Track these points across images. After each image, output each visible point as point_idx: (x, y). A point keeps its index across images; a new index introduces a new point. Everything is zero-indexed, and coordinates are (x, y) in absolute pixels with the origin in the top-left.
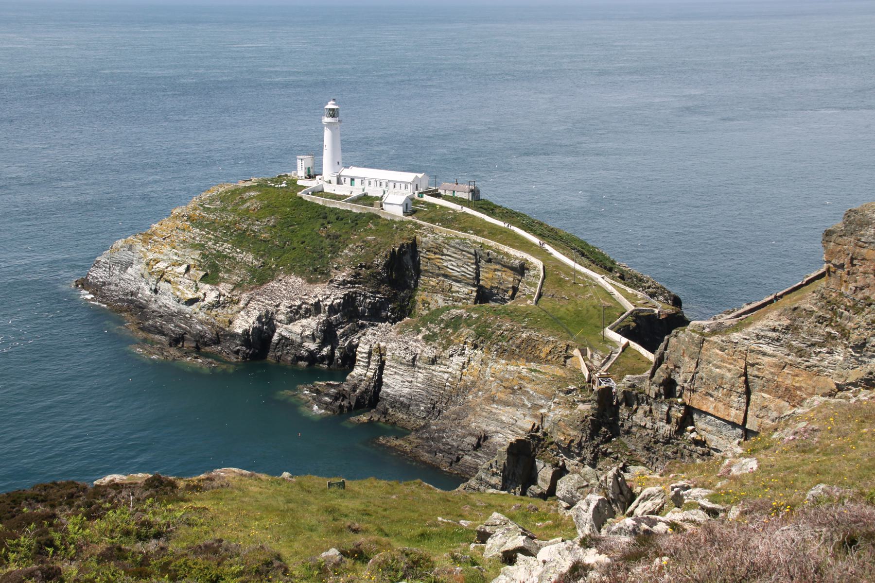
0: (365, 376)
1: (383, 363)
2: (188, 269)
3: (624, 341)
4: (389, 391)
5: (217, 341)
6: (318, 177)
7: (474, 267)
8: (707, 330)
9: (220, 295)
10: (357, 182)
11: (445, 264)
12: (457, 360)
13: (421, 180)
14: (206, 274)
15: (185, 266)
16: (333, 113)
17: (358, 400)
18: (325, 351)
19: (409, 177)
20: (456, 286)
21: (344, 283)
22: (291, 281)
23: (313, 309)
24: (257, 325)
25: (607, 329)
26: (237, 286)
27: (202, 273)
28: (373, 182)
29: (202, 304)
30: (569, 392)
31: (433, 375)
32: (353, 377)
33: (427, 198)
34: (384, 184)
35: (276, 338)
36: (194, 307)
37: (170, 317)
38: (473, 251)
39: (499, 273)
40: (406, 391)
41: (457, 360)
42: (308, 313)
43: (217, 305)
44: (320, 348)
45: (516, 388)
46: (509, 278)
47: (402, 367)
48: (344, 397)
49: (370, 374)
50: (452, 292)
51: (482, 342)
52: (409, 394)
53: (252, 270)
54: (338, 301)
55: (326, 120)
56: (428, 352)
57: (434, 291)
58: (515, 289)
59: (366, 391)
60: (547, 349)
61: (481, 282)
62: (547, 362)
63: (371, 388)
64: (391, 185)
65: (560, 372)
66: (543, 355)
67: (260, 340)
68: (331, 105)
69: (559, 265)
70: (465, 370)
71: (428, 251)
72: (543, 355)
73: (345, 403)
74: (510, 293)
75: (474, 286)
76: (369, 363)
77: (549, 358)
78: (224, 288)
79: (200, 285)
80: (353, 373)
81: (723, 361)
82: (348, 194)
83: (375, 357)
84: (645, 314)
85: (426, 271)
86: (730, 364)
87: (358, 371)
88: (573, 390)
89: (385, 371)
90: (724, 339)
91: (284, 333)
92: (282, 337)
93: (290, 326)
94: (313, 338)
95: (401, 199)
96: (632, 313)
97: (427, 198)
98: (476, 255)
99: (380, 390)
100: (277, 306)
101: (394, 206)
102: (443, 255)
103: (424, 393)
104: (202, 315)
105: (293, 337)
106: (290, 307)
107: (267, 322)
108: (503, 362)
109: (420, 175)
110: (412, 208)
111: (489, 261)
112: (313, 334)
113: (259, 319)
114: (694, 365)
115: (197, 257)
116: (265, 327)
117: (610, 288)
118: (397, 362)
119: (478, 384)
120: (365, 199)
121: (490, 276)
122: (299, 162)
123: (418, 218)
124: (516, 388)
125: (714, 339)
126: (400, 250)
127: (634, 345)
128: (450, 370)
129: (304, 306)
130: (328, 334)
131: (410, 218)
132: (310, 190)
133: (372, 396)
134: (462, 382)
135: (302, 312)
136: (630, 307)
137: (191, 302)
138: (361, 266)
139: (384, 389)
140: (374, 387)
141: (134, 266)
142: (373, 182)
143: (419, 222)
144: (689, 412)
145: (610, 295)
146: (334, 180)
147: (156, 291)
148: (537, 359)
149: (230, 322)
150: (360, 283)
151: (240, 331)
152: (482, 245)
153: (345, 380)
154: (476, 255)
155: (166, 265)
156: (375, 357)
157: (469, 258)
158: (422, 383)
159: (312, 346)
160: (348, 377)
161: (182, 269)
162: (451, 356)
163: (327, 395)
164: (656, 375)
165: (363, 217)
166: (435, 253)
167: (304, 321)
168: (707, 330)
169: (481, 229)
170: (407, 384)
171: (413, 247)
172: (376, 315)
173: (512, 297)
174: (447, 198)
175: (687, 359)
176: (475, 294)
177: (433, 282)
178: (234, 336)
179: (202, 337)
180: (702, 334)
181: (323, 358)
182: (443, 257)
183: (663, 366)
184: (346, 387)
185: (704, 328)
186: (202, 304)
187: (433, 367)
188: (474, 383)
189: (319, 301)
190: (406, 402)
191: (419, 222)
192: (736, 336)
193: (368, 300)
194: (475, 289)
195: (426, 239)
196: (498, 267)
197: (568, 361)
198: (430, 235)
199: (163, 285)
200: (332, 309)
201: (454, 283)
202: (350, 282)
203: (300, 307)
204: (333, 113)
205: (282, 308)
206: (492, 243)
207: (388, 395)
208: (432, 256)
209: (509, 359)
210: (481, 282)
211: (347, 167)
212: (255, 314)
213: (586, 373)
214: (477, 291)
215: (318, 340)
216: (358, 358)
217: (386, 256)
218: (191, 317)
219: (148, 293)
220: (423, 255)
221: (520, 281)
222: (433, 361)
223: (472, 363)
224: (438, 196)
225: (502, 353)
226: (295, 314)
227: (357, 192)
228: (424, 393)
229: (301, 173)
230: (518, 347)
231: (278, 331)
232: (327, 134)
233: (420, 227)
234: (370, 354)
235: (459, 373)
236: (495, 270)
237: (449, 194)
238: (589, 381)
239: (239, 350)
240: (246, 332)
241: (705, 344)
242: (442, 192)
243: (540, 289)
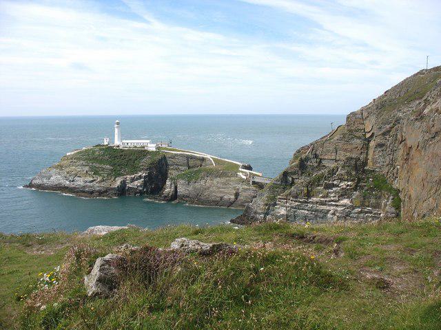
3: (248, 171)
5: (106, 191)
10: (129, 144)
16: (118, 124)
20: (180, 167)
35: (127, 188)
36: (94, 183)
42: (137, 179)
44: (143, 189)
46: (199, 162)
68: (117, 121)
87: (167, 190)
92: (129, 187)
94: (141, 186)
101: (152, 147)
107: (124, 183)
127: (250, 171)
133: (175, 196)
137: (92, 181)
144: (321, 159)
159: (141, 189)
165: (143, 153)
171: (165, 157)
195: (167, 156)
204: (118, 124)
232: (116, 130)
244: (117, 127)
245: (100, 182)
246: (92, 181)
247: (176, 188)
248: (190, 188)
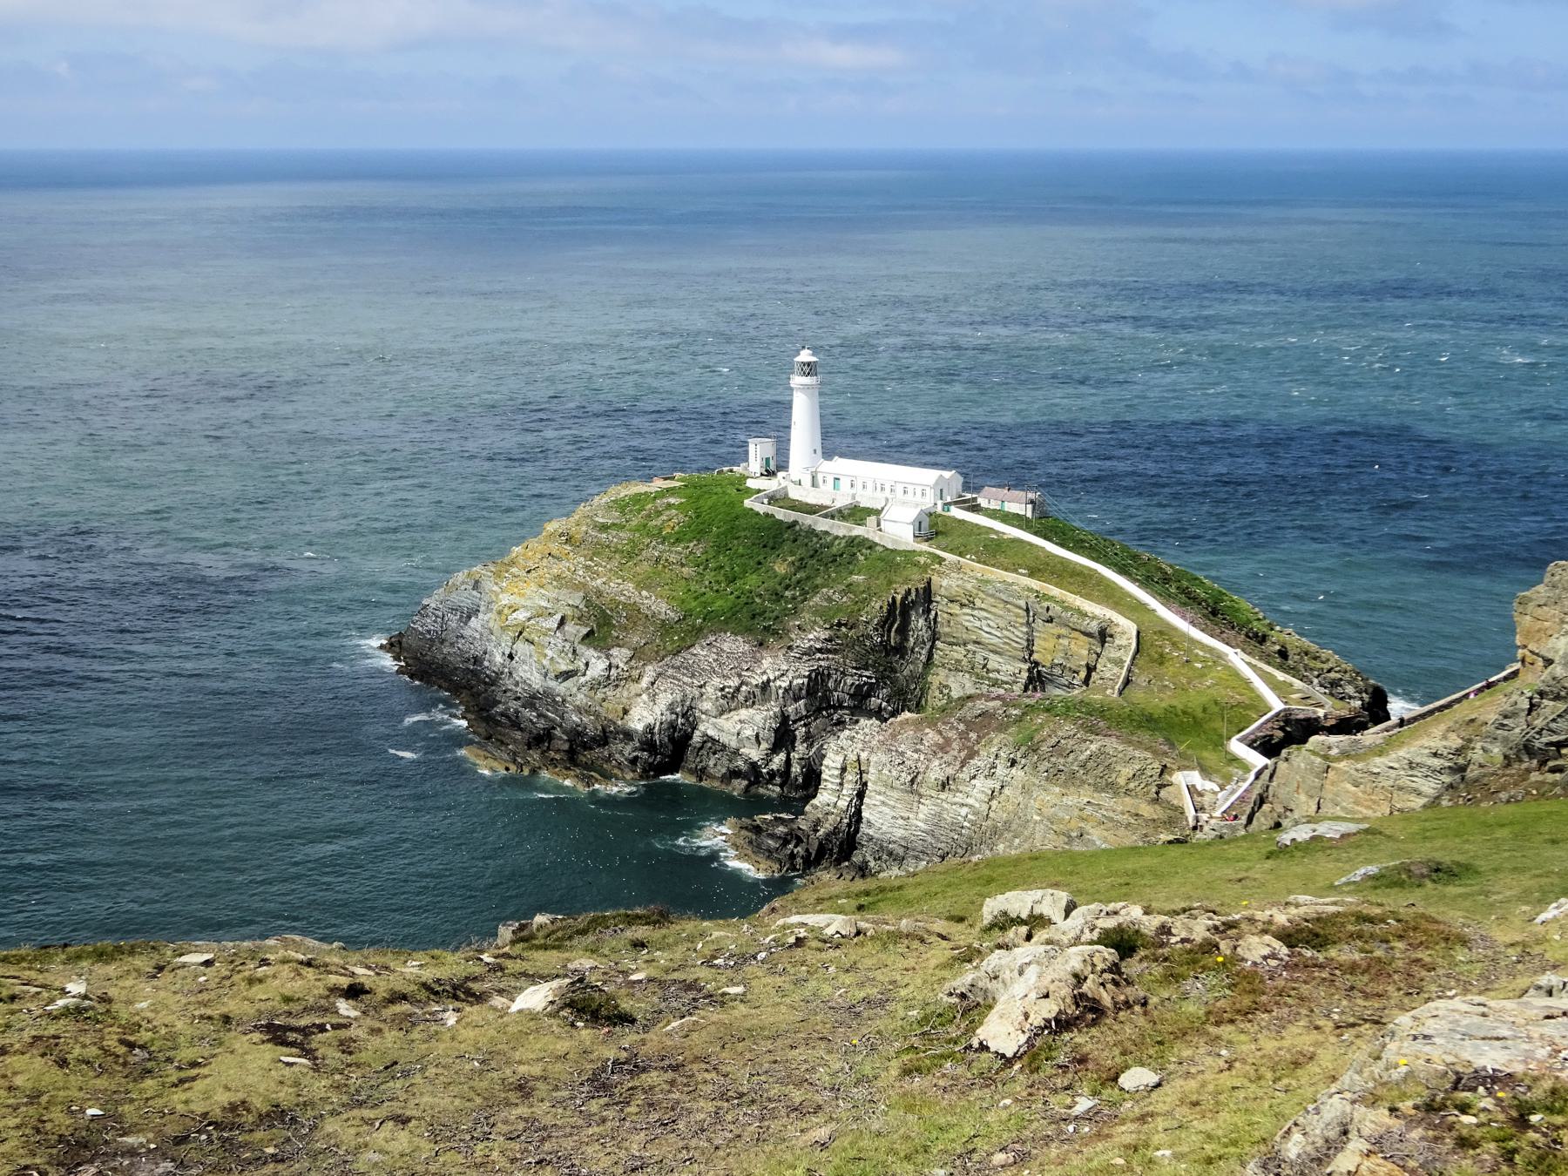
0: (835, 805)
1: (865, 784)
2: (562, 622)
4: (871, 832)
6: (781, 474)
7: (1025, 629)
8: (1334, 752)
9: (610, 666)
10: (844, 484)
11: (978, 624)
12: (982, 785)
13: (948, 482)
14: (590, 634)
15: (558, 617)
17: (820, 844)
18: (778, 761)
19: (930, 476)
21: (810, 652)
22: (726, 647)
23: (758, 692)
24: (670, 717)
25: (1234, 739)
26: (637, 654)
27: (585, 631)
28: (870, 485)
29: (583, 679)
31: (943, 809)
32: (816, 807)
33: (957, 513)
34: (888, 488)
37: (532, 700)
38: (1022, 603)
39: (1065, 642)
40: (899, 833)
41: (982, 785)
42: (751, 701)
43: (606, 681)
45: (1074, 834)
46: (1081, 650)
47: (895, 794)
48: (799, 841)
49: (843, 804)
50: (988, 671)
51: (1024, 756)
52: (904, 838)
53: (665, 628)
54: (800, 681)
55: (797, 380)
56: (936, 772)
57: (957, 668)
58: (1091, 669)
59: (836, 831)
60: (1127, 771)
61: (1035, 657)
62: (1128, 792)
63: (844, 827)
64: (899, 489)
65: (1147, 810)
66: (1122, 781)
67: (674, 744)
68: (805, 356)
69: (1166, 631)
70: (994, 803)
72: (1122, 781)
73: (800, 850)
74: (1083, 674)
75: (1024, 660)
76: (841, 784)
77: (1132, 785)
78: (620, 655)
79: (581, 649)
80: (815, 801)
81: (1357, 803)
82: (828, 503)
83: (850, 777)
84: (1301, 716)
85: (947, 635)
86: (1368, 807)
87: (823, 797)
89: (866, 800)
90: (1359, 766)
91: (711, 732)
92: (708, 739)
93: (721, 721)
95: (912, 514)
96: (1277, 714)
97: (957, 513)
98: (1027, 610)
99: (857, 831)
103: (929, 839)
104: (581, 699)
105: (724, 739)
106: (722, 689)
108: (1057, 790)
109: (947, 474)
110: (933, 528)
111: (1050, 620)
112: (757, 736)
113: (671, 708)
114: (1315, 807)
115: (577, 602)
116: (680, 721)
117: (1248, 673)
118: (886, 786)
119: (1014, 826)
120: (856, 513)
121: (1050, 645)
122: (751, 448)
123: (938, 547)
124: (1074, 834)
125: (1342, 765)
126: (905, 598)
128: (970, 801)
129: (744, 688)
130: (783, 738)
131: (924, 547)
132: (767, 496)
134: (989, 822)
135: (741, 698)
136: (1277, 705)
137: (567, 675)
138: (839, 624)
139: (864, 828)
140: (849, 825)
141: (481, 615)
142: (870, 485)
143: (938, 552)
145: (1247, 683)
146: (807, 481)
147: (511, 657)
148: (1111, 787)
149: (626, 712)
150: (835, 652)
151: (640, 727)
152: (1040, 596)
153: (803, 813)
155: (528, 615)
156: (850, 777)
157: (1017, 616)
158: (925, 821)
159: (755, 754)
160: (808, 808)
161: (553, 623)
163: (772, 836)
164: (1255, 822)
166: (962, 605)
167: (744, 713)
168: (1334, 752)
169: (1041, 568)
170: (901, 822)
171: (927, 594)
172: (860, 703)
173: (1086, 682)
174: (993, 514)
175: (1303, 797)
176: (1025, 675)
177: (958, 653)
178: (628, 735)
179: (579, 734)
180: (1326, 757)
181: (772, 774)
182: (975, 612)
183: (1266, 807)
184: (803, 824)
185: (1330, 748)
186: (583, 679)
187: (943, 796)
188: (1008, 823)
189: (769, 681)
190: (901, 851)
191: (938, 552)
192: (1378, 763)
193: (849, 681)
194: (1026, 666)
195: (945, 584)
196: (1063, 631)
198: (955, 576)
199: (522, 648)
200: (792, 694)
201: (992, 656)
202: (820, 651)
203: (738, 689)
204: (809, 370)
205: (709, 689)
206: (1055, 591)
207: (871, 839)
208: (955, 609)
209: (1065, 785)
210: (1035, 657)
211: (828, 454)
212: (664, 699)
213: (1190, 813)
214: (1029, 670)
215: (764, 745)
216: (824, 776)
218: (564, 701)
219: (499, 659)
220: (940, 606)
221: (1099, 655)
222: (944, 786)
223: (1006, 791)
224: (975, 508)
225: (1054, 775)
226: (730, 701)
227: (842, 502)
229: (755, 466)
230: (1083, 766)
231: (702, 727)
233: (941, 560)
234: (844, 770)
235: (985, 807)
236: (1059, 637)
237: (994, 505)
238: (1195, 828)
239: (636, 758)
240: (650, 729)
241: (1331, 774)
242: (983, 502)
243: (1129, 671)
244: (805, 387)
245: (595, 686)
246: (567, 675)
247: (861, 795)
248: (924, 813)
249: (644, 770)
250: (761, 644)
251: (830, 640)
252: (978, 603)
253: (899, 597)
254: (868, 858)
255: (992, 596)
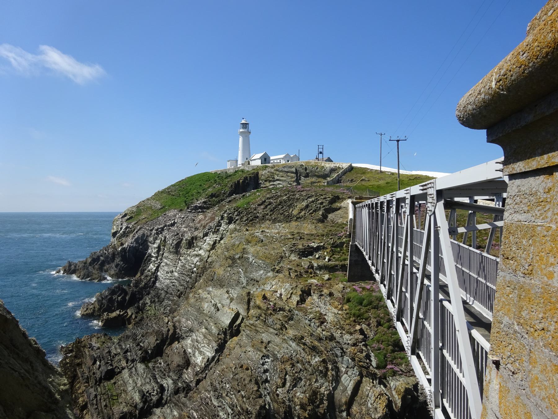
12: (210, 239)
30: (307, 252)
38: (294, 170)
41: (210, 239)
45: (237, 257)
66: (295, 212)
71: (266, 181)
76: (157, 257)
88: (318, 249)
100: (151, 230)
102: (274, 181)
111: (307, 176)
126: (243, 182)
154: (296, 172)
157: (292, 178)
162: (206, 235)
166: (270, 181)
197: (330, 216)
202: (200, 207)
217: (232, 186)
223: (222, 242)
228: (177, 284)
235: (207, 253)
249: (120, 270)
250: (181, 210)
251: (204, 202)
252: (276, 177)
253: (241, 181)
254: (148, 301)
255: (282, 171)
